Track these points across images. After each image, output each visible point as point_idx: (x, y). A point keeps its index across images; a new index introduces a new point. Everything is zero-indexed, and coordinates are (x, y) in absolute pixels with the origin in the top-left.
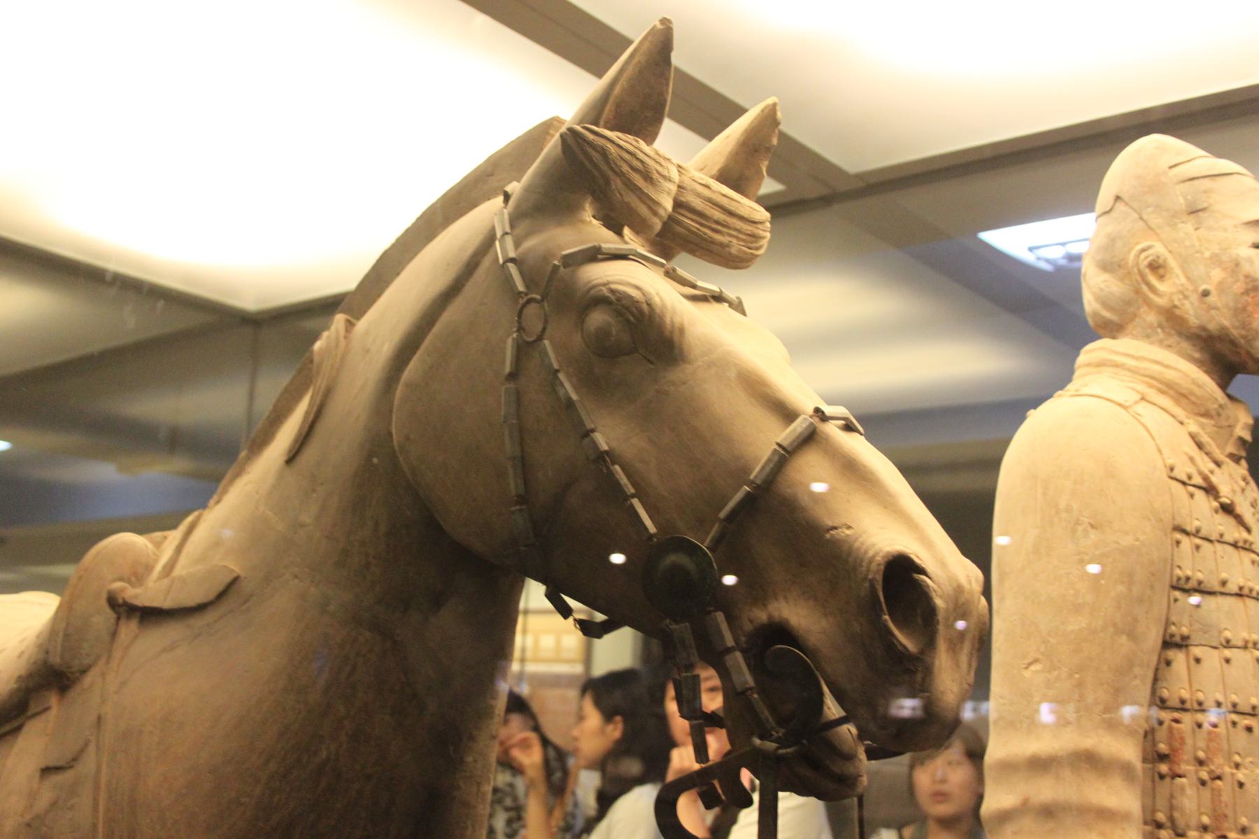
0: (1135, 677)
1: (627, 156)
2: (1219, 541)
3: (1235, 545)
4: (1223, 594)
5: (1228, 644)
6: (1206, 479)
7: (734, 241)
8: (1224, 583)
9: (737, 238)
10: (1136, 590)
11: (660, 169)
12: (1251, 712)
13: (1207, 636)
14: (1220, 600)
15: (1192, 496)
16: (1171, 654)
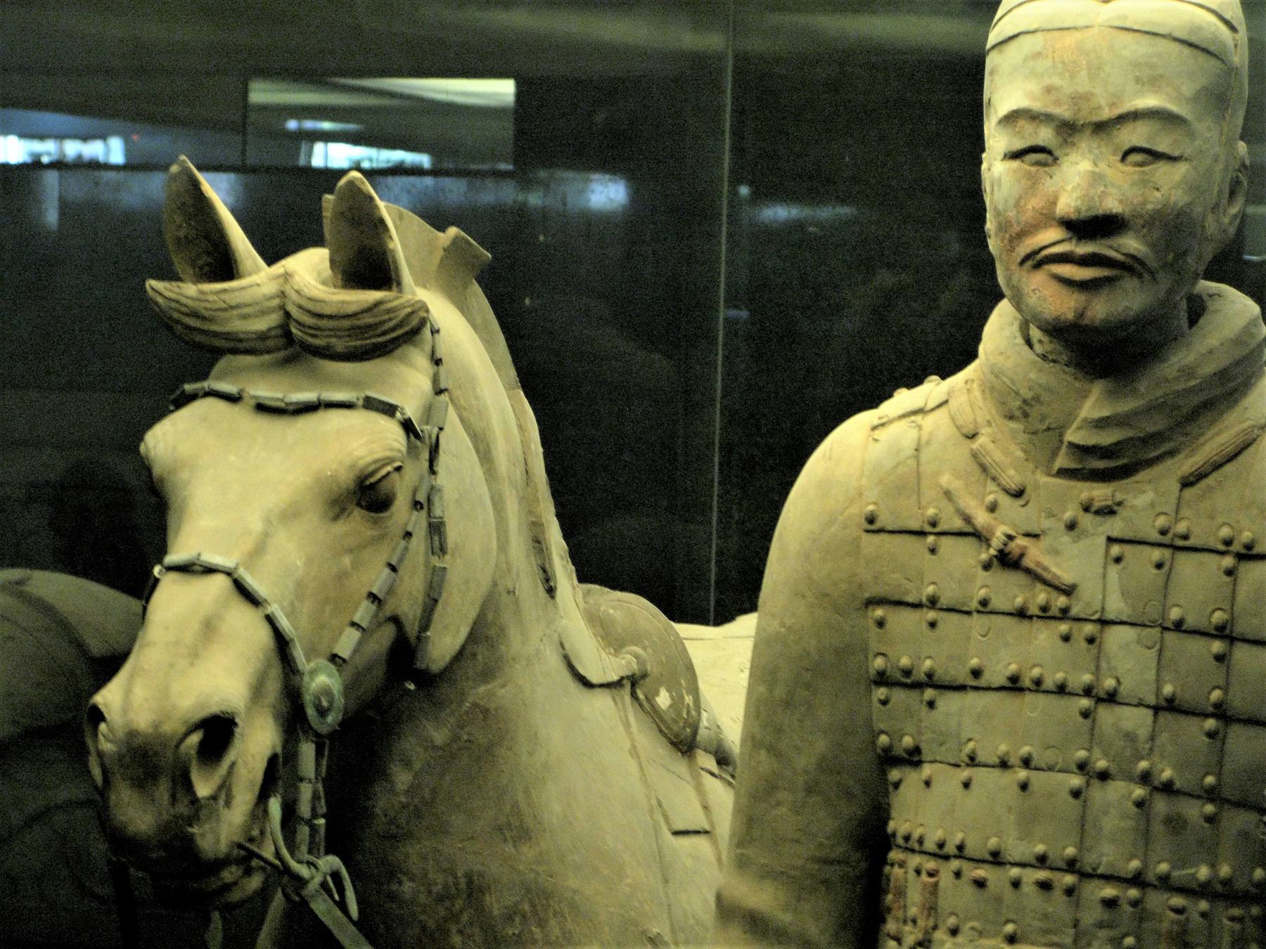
0: (779, 804)
1: (173, 305)
2: (979, 612)
3: (1021, 614)
4: (976, 688)
5: (972, 761)
6: (968, 519)
7: (334, 340)
8: (976, 673)
9: (335, 336)
10: (780, 691)
11: (209, 306)
12: (989, 858)
13: (943, 749)
14: (971, 697)
15: (933, 551)
16: (894, 774)
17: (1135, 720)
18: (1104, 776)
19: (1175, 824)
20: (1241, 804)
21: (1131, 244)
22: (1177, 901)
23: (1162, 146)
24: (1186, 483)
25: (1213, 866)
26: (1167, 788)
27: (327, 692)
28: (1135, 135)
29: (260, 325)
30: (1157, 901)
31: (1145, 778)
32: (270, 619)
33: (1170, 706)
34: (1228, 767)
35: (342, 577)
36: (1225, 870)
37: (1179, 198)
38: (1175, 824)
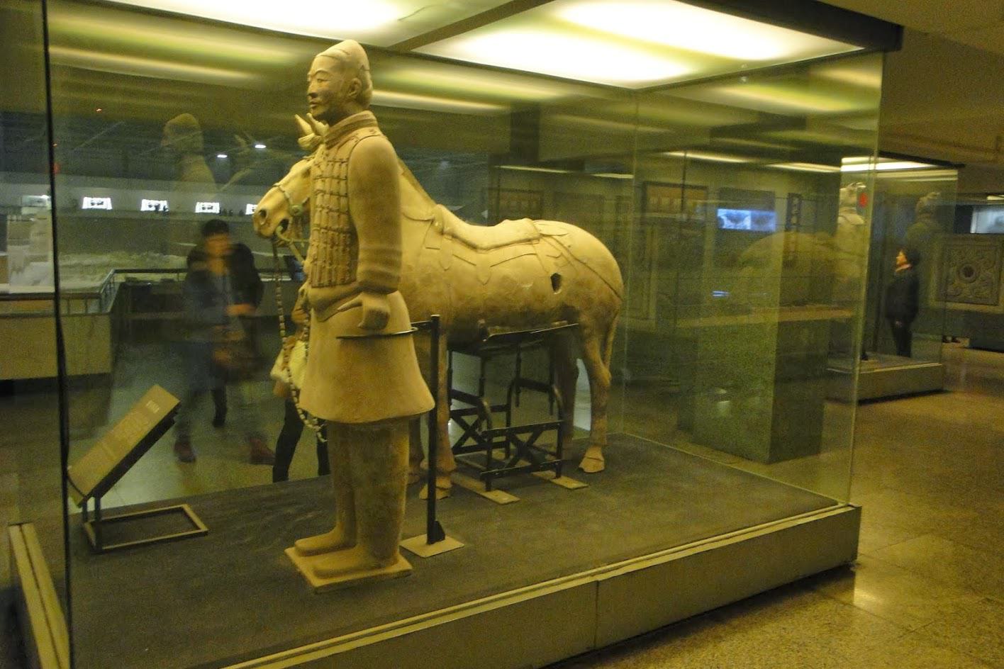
17: (327, 196)
18: (323, 208)
19: (332, 217)
20: (344, 213)
21: (318, 99)
22: (332, 232)
23: (323, 78)
24: (339, 147)
25: (339, 225)
26: (331, 210)
27: (296, 208)
28: (319, 76)
29: (308, 145)
30: (331, 233)
31: (328, 208)
32: (285, 195)
33: (331, 194)
34: (342, 205)
35: (305, 188)
36: (341, 226)
37: (326, 88)
38: (332, 217)
